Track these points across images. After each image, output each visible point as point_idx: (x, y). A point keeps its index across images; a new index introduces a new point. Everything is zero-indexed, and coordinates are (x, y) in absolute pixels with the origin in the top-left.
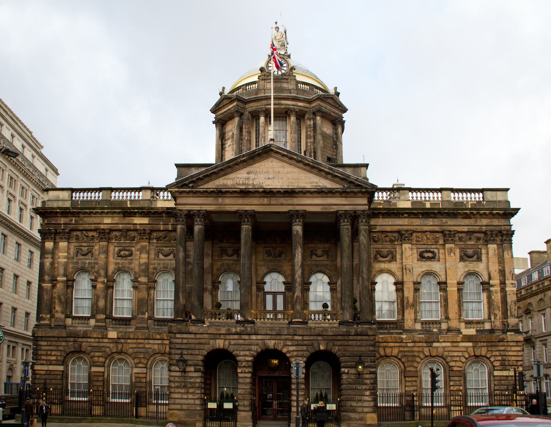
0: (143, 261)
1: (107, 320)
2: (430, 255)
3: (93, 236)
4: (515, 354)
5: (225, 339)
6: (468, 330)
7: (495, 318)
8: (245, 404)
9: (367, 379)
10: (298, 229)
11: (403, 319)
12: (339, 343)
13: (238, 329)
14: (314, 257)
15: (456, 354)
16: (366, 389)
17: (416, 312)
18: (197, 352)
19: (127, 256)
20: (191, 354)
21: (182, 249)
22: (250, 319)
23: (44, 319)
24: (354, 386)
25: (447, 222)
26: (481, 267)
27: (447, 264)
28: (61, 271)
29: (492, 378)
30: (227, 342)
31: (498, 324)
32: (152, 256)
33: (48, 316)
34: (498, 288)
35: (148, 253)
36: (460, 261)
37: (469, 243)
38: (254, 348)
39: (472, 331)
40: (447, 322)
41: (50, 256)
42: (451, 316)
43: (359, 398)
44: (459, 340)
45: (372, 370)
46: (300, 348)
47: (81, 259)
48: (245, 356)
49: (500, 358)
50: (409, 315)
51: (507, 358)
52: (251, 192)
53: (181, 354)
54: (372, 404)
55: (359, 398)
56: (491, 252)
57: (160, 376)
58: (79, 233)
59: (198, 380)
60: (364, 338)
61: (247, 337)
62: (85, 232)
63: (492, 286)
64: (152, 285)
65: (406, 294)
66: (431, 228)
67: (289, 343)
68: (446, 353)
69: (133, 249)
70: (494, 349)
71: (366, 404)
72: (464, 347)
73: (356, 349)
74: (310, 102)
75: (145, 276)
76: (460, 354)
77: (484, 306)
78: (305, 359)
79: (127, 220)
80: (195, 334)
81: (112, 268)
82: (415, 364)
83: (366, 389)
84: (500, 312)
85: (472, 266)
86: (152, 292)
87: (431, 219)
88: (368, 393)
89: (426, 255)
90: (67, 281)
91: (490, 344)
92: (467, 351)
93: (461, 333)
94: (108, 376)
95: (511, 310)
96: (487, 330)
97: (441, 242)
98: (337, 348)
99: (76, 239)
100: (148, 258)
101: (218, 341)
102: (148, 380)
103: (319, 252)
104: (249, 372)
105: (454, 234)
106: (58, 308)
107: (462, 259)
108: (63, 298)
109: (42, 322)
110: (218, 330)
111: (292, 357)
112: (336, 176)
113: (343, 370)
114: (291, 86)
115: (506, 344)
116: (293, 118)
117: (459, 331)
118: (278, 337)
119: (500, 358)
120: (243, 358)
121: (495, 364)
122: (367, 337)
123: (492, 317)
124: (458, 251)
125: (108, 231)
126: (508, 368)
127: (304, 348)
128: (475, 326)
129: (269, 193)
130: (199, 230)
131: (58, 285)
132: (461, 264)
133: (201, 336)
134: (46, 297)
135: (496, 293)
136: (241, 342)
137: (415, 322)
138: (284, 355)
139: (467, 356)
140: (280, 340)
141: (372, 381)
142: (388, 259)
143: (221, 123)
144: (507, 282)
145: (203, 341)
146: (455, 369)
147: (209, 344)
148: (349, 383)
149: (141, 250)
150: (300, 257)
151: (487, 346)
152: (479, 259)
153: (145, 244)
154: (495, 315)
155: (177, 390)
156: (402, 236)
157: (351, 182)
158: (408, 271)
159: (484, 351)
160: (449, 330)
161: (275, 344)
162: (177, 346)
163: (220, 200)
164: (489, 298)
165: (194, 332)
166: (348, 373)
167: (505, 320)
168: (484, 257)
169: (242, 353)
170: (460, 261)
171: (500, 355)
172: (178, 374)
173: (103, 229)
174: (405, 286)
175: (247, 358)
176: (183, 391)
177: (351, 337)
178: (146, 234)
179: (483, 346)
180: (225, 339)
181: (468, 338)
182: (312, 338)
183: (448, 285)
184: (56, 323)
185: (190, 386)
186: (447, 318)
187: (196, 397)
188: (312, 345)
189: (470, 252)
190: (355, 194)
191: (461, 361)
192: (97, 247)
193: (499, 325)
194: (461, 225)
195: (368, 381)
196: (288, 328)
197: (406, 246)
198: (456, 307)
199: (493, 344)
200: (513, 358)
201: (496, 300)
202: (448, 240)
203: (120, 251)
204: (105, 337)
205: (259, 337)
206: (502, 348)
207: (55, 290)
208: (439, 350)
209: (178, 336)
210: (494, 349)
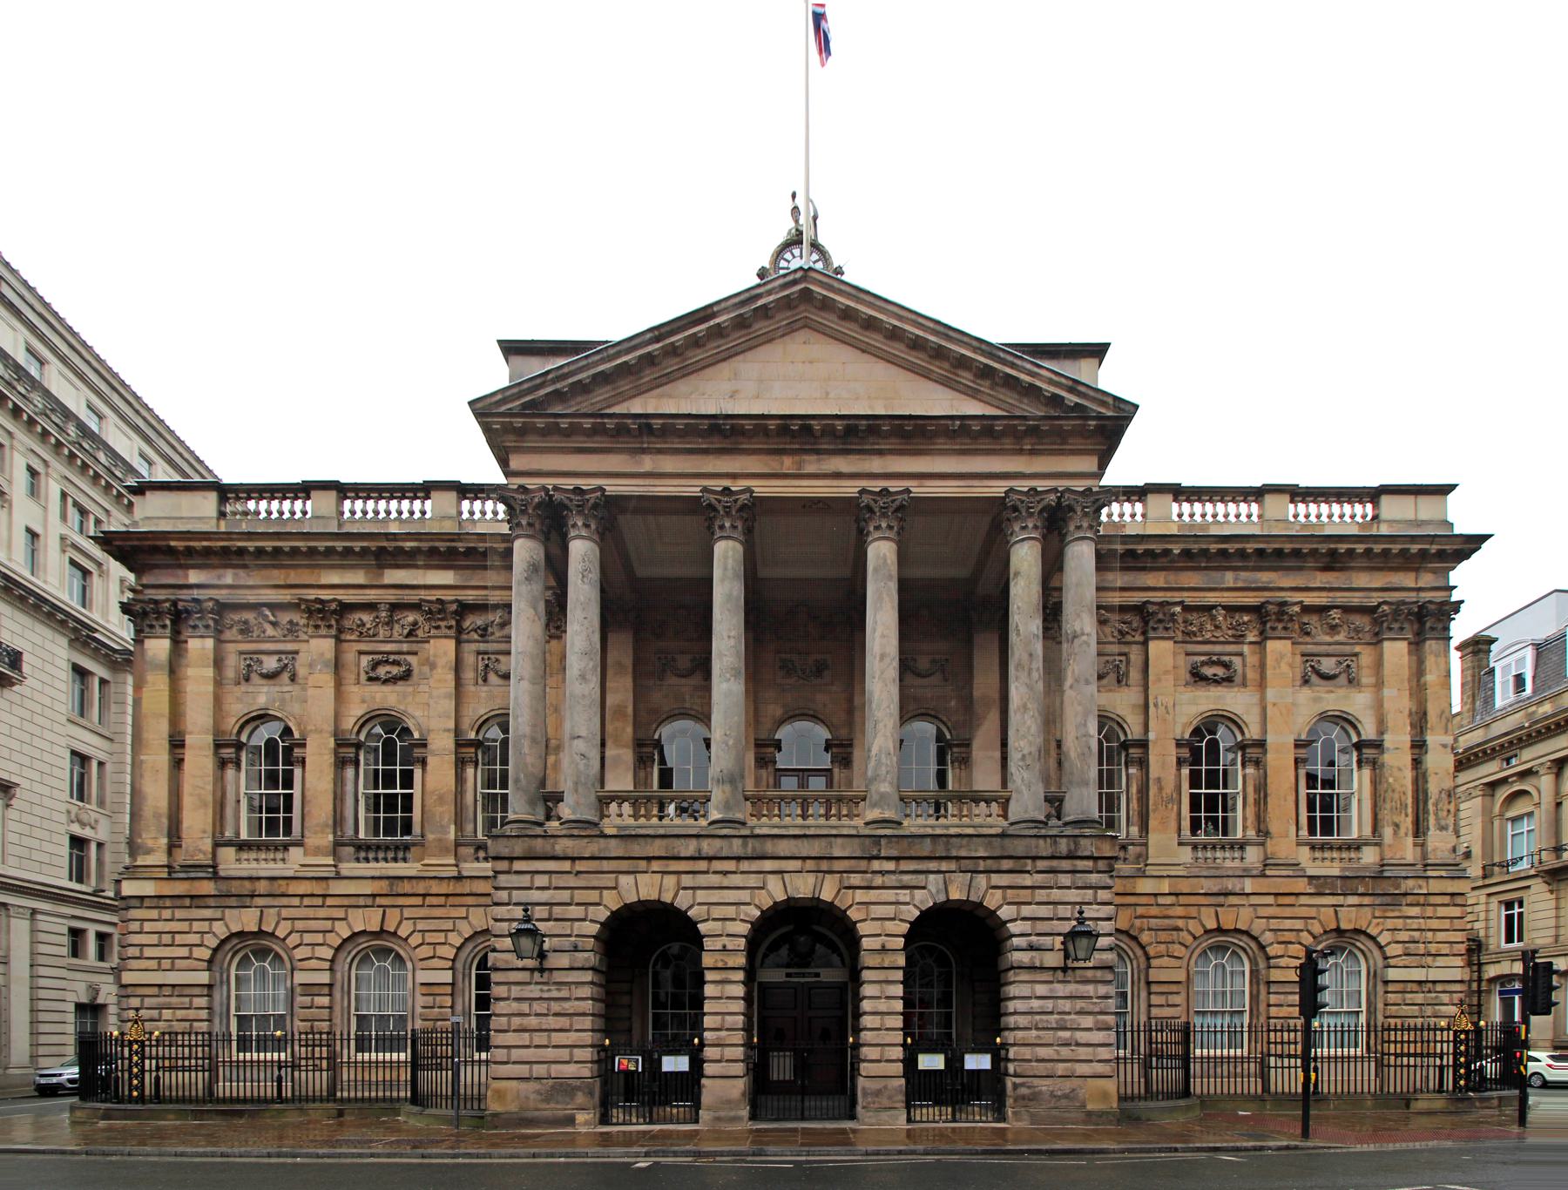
3: (291, 622)
40: (1263, 844)
58: (249, 616)
85: (1335, 699)
99: (242, 632)
125: (334, 606)
183: (1269, 746)
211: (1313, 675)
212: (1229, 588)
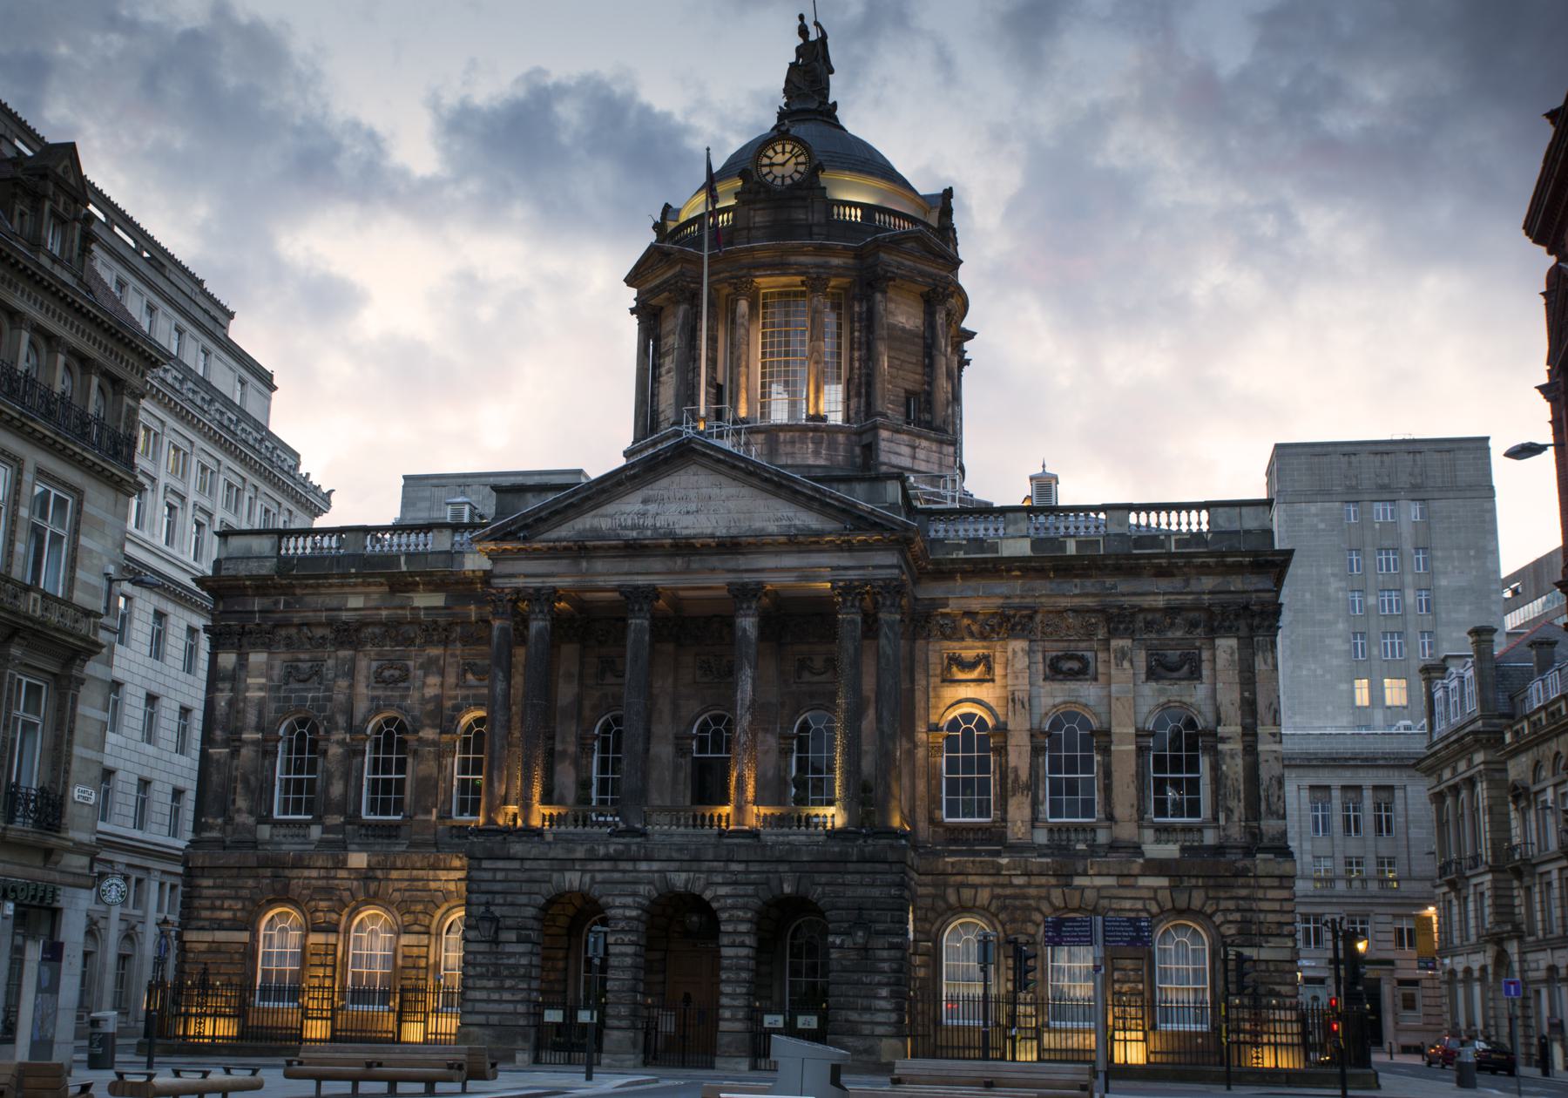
0: (430, 692)
1: (349, 827)
2: (1075, 665)
4: (1277, 906)
5: (584, 871)
6: (1160, 846)
7: (1228, 818)
8: (619, 1011)
9: (884, 960)
10: (748, 624)
11: (1004, 820)
12: (824, 879)
13: (611, 850)
14: (807, 676)
16: (880, 984)
18: (523, 899)
19: (396, 681)
20: (512, 904)
21: (500, 675)
22: (638, 826)
23: (211, 828)
24: (855, 977)
25: (1115, 587)
26: (1198, 694)
27: (1114, 688)
28: (251, 718)
31: (1236, 832)
33: (220, 821)
34: (1237, 746)
35: (442, 673)
37: (1170, 635)
38: (642, 889)
39: (1170, 850)
41: (228, 685)
43: (865, 1002)
44: (1136, 869)
45: (897, 940)
46: (741, 890)
47: (296, 691)
48: (624, 907)
49: (1237, 916)
51: (1255, 917)
52: (646, 546)
53: (487, 904)
54: (894, 1017)
55: (865, 1002)
56: (1222, 657)
58: (293, 631)
60: (879, 867)
61: (629, 866)
62: (305, 629)
63: (1223, 740)
65: (1013, 760)
66: (1077, 601)
67: (719, 879)
68: (1105, 903)
69: (411, 663)
70: (1222, 894)
71: (880, 1017)
72: (1148, 888)
73: (861, 891)
75: (433, 727)
76: (1139, 905)
79: (399, 599)
80: (522, 859)
83: (880, 984)
84: (1242, 804)
85: (1175, 691)
87: (1077, 581)
88: (884, 992)
89: (1067, 665)
90: (265, 740)
91: (1212, 882)
92: (1155, 899)
93: (1142, 854)
94: (346, 952)
95: (1267, 800)
96: (1209, 847)
97: (1101, 633)
98: (820, 889)
99: (287, 645)
100: (442, 685)
101: (568, 875)
102: (432, 961)
103: (818, 663)
104: (632, 943)
105: (1133, 614)
106: (241, 803)
107: (1151, 675)
108: (252, 778)
109: (206, 835)
110: (569, 851)
111: (724, 909)
112: (828, 504)
113: (831, 939)
115: (1252, 881)
117: (1137, 849)
118: (695, 866)
119: (1237, 916)
120: (620, 911)
121: (1223, 929)
122: (886, 867)
123: (1222, 817)
124: (1141, 658)
126: (1257, 940)
127: (750, 889)
128: (1181, 836)
129: (683, 548)
130: (540, 632)
131: (244, 751)
132: (1150, 689)
133: (534, 865)
135: (1232, 757)
136: (617, 876)
137: (1033, 827)
138: (707, 904)
139: (1154, 909)
140: (700, 872)
141: (895, 966)
142: (975, 675)
143: (648, 315)
144: (1260, 730)
145: (537, 875)
147: (550, 882)
148: (845, 970)
149: (429, 666)
150: (749, 688)
151: (1205, 887)
152: (1195, 675)
153: (434, 651)
154: (1229, 811)
155: (479, 983)
157: (860, 517)
158: (1018, 706)
159: (1197, 900)
160: (1114, 846)
161: (687, 881)
162: (484, 887)
165: (520, 855)
166: (841, 947)
167: (1255, 824)
168: (1206, 671)
169: (618, 901)
171: (1238, 910)
172: (483, 947)
173: (345, 623)
175: (628, 913)
176: (491, 984)
177: (851, 867)
178: (435, 630)
179: (1197, 887)
180: (584, 871)
181: (1158, 867)
182: (765, 867)
183: (1114, 738)
184: (237, 837)
185: (506, 973)
186: (1110, 817)
187: (519, 997)
188: (767, 883)
189: (1173, 655)
192: (331, 662)
193: (1237, 836)
194: (1155, 594)
195: (885, 966)
196: (716, 846)
198: (1133, 791)
199: (1222, 881)
200: (1271, 918)
201: (1231, 775)
202: (1116, 629)
204: (343, 865)
205: (656, 866)
206: (1243, 892)
207: (235, 762)
208: (1088, 893)
209: (486, 864)
210: (1222, 894)
211: (1159, 670)
212: (1075, 594)
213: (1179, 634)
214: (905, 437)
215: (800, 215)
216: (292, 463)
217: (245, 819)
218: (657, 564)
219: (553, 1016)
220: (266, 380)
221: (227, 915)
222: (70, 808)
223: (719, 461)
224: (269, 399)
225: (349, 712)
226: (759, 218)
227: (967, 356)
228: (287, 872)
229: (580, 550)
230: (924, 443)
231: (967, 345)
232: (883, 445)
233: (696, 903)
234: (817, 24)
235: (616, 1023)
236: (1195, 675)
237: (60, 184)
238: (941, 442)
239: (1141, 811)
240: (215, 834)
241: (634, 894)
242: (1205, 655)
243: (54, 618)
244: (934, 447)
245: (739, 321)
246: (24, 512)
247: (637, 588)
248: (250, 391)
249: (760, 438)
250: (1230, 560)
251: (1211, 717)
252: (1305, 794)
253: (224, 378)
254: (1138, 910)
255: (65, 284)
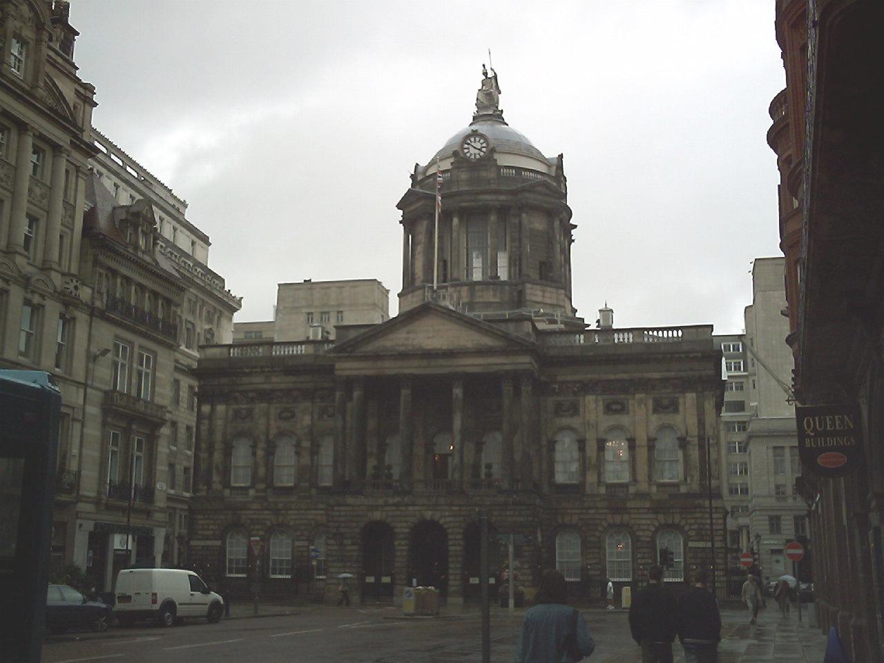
2: (619, 407)
7: (691, 480)
10: (458, 392)
12: (496, 513)
15: (644, 522)
17: (599, 475)
18: (354, 525)
26: (677, 420)
29: (687, 550)
30: (384, 513)
31: (695, 487)
32: (316, 416)
33: (205, 487)
36: (653, 413)
41: (206, 422)
42: (639, 478)
50: (591, 478)
57: (321, 548)
59: (355, 554)
61: (404, 508)
64: (315, 450)
74: (512, 193)
76: (649, 522)
77: (680, 468)
78: (462, 531)
81: (273, 431)
82: (598, 534)
84: (698, 473)
85: (667, 418)
86: (316, 457)
89: (614, 407)
94: (269, 549)
106: (216, 478)
107: (655, 411)
108: (221, 467)
114: (492, 174)
116: (493, 218)
119: (696, 527)
124: (650, 403)
127: (462, 519)
134: (203, 466)
136: (398, 513)
137: (598, 486)
146: (643, 539)
154: (692, 476)
155: (335, 564)
156: (587, 388)
163: (379, 364)
164: (686, 457)
168: (681, 408)
170: (653, 413)
172: (335, 548)
174: (588, 444)
176: (339, 565)
186: (635, 480)
189: (666, 402)
190: (516, 353)
191: (650, 530)
192: (257, 410)
195: (527, 554)
197: (590, 398)
198: (646, 468)
203: (282, 412)
205: (417, 508)
206: (699, 515)
209: (336, 508)
211: (659, 408)
213: (668, 391)
214: (538, 287)
215: (484, 174)
216: (221, 285)
217: (217, 486)
218: (416, 363)
219: (371, 579)
220: (205, 240)
221: (211, 532)
222: (157, 493)
223: (443, 313)
224: (208, 250)
225: (267, 435)
226: (464, 176)
227: (573, 238)
228: (238, 512)
229: (377, 357)
230: (549, 289)
231: (573, 232)
232: (528, 291)
233: (434, 525)
234: (492, 69)
235: (400, 582)
236: (676, 410)
237: (145, 219)
238: (557, 288)
239: (650, 477)
240: (204, 494)
241: (406, 522)
242: (681, 401)
243: (149, 411)
244: (554, 290)
245: (454, 228)
246: (135, 365)
247: (405, 375)
248: (197, 247)
249: (465, 288)
250: (692, 355)
251: (684, 434)
252: (771, 452)
253: (184, 241)
254: (649, 525)
255: (148, 263)
